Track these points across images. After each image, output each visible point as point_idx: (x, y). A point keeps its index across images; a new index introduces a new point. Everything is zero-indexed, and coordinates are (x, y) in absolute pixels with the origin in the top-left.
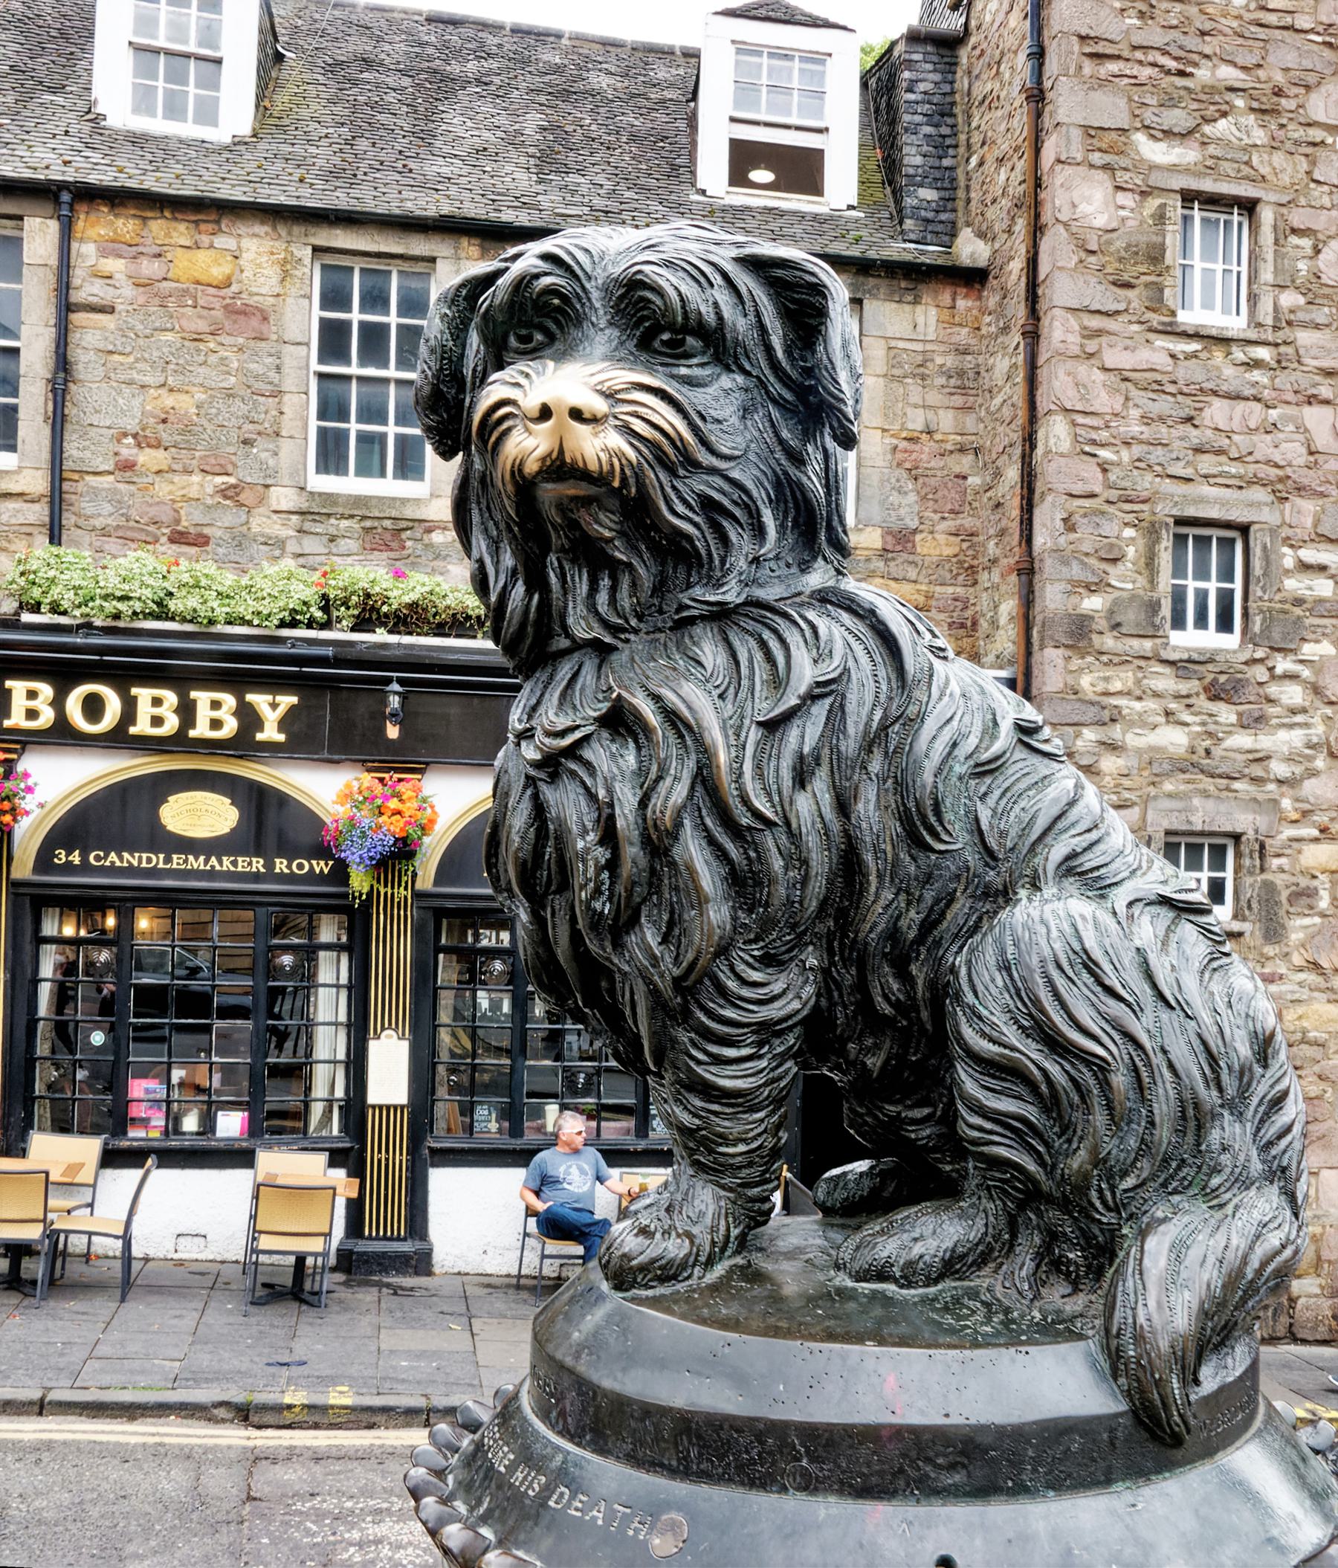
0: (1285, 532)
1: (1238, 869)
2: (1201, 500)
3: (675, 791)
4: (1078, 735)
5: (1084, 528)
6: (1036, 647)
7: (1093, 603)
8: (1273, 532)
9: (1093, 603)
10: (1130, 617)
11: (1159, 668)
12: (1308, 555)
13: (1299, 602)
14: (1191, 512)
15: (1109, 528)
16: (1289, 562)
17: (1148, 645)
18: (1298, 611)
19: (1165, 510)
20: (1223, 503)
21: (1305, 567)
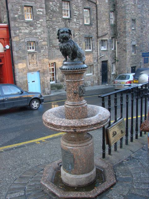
0: (36, 7)
1: (35, 45)
2: (27, 3)
3: (70, 47)
4: (16, 31)
5: (14, 7)
6: (10, 21)
7: (16, 16)
8: (35, 7)
9: (16, 16)
10: (21, 17)
11: (24, 23)
12: (39, 10)
13: (39, 15)
14: (26, 5)
15: (17, 7)
16: (37, 10)
17: (23, 20)
18: (39, 16)
19: (23, 5)
20: (29, 4)
21: (39, 11)
